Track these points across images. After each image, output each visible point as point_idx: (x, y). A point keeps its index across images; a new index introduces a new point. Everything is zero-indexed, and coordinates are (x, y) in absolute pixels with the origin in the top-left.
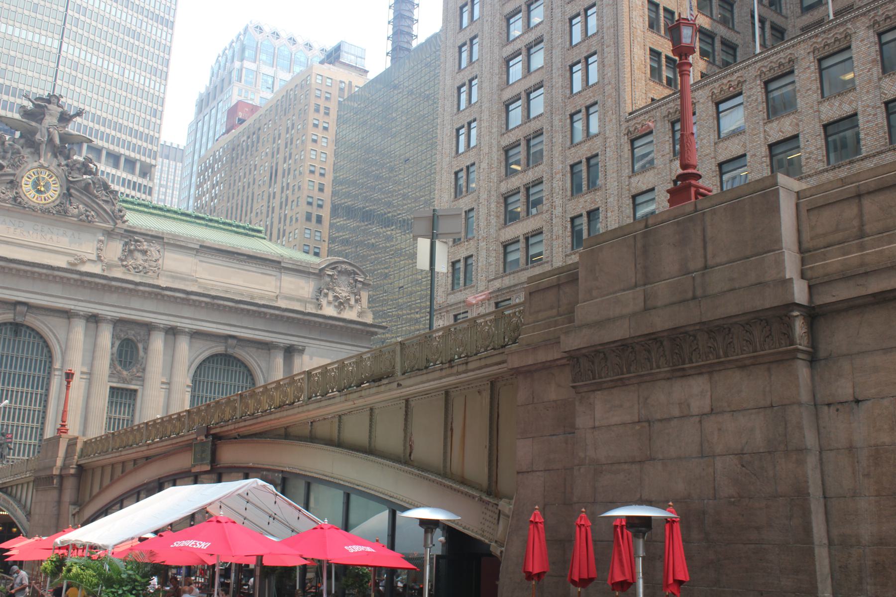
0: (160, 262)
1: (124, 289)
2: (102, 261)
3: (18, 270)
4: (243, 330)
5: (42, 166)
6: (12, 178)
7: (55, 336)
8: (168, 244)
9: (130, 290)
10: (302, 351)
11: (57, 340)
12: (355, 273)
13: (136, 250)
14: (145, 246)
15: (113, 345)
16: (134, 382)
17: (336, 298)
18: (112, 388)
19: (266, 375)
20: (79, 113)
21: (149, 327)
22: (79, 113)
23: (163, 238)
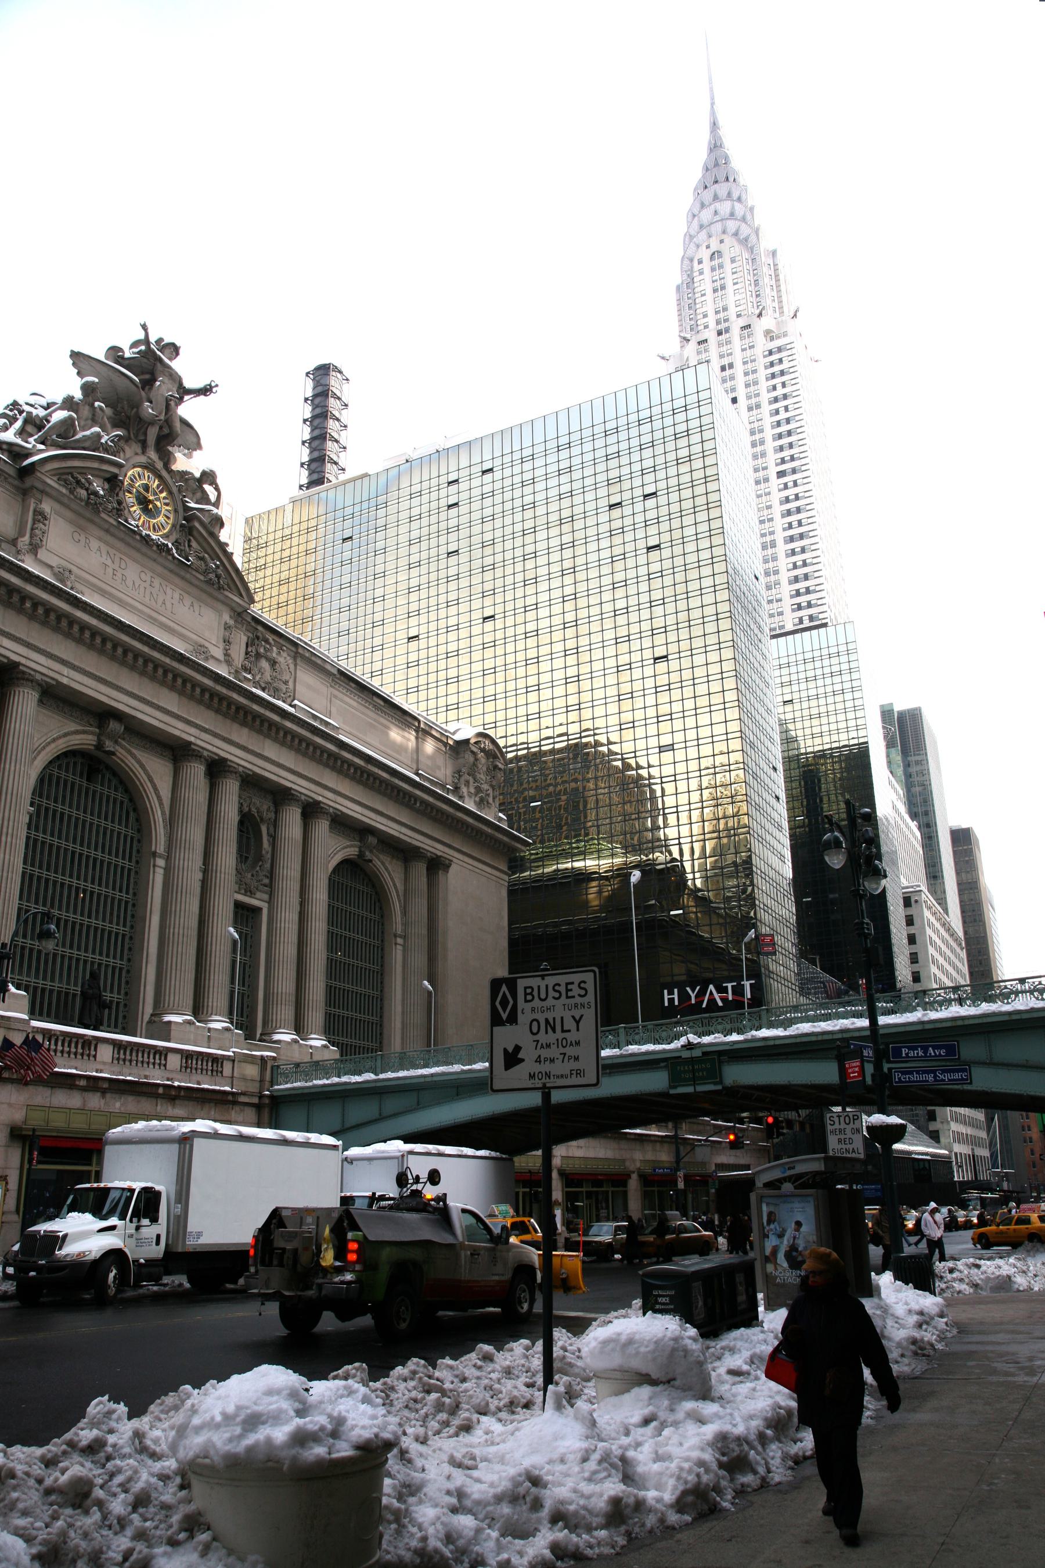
1: (263, 720)
3: (127, 650)
5: (149, 467)
6: (115, 470)
8: (303, 657)
9: (272, 724)
11: (159, 798)
12: (495, 757)
16: (258, 895)
17: (478, 790)
20: (206, 391)
22: (206, 391)
23: (295, 645)
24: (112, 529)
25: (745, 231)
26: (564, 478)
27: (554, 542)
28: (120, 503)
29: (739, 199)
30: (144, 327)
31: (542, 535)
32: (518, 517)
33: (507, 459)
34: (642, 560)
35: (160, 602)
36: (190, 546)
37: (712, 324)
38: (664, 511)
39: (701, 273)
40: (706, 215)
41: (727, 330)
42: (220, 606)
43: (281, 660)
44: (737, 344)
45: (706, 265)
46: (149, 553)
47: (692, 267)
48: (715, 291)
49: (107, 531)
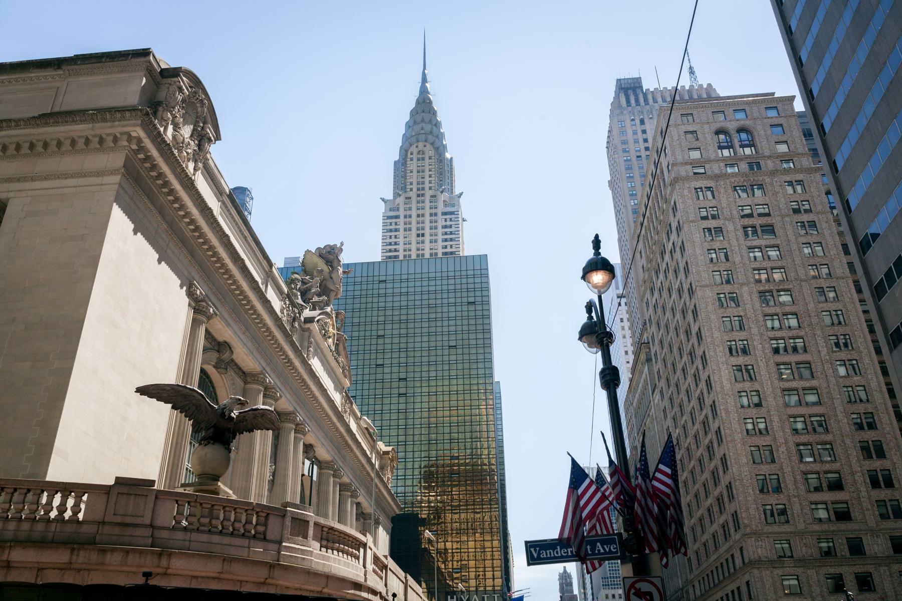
25: (437, 143)
26: (403, 298)
27: (396, 332)
29: (436, 125)
30: (342, 244)
31: (389, 327)
32: (375, 313)
33: (370, 279)
34: (446, 352)
37: (415, 190)
38: (459, 328)
39: (412, 159)
40: (417, 128)
41: (423, 195)
44: (427, 205)
45: (415, 157)
47: (406, 155)
48: (418, 172)
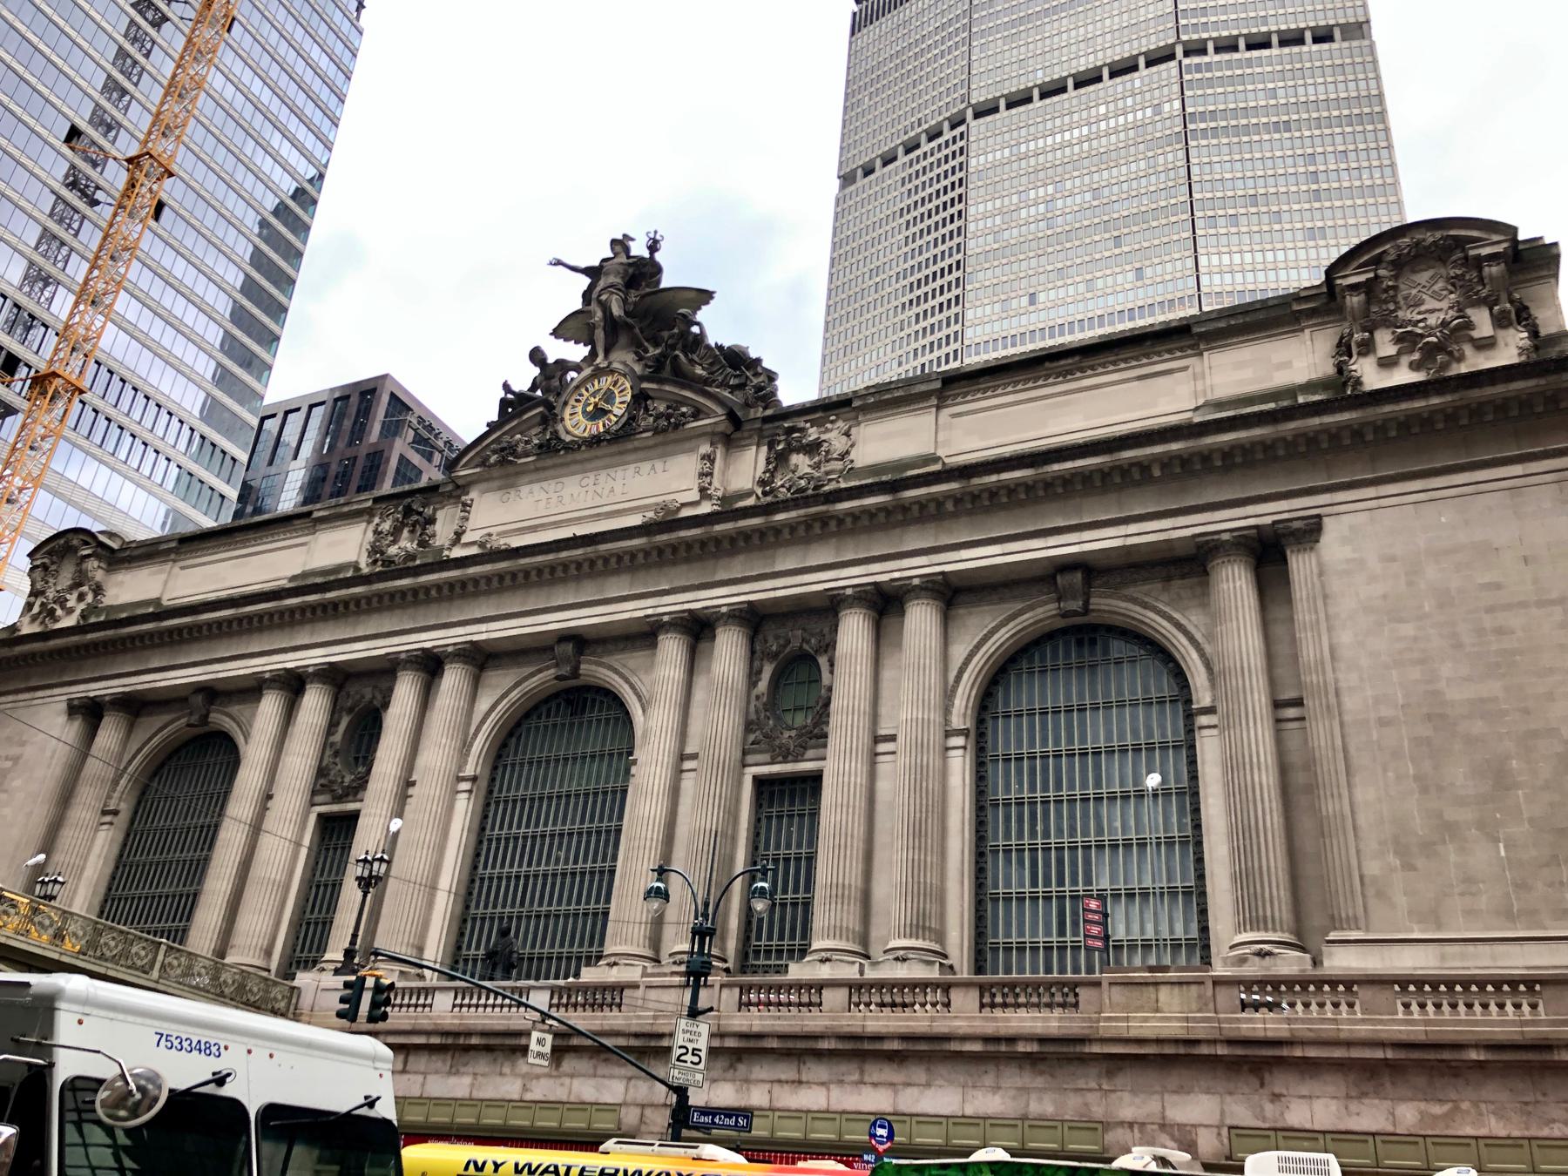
0: (852, 457)
2: (710, 497)
4: (1087, 535)
6: (541, 409)
7: (632, 687)
9: (761, 533)
10: (1310, 531)
12: (1461, 243)
13: (790, 450)
14: (813, 434)
15: (753, 676)
16: (810, 753)
17: (1407, 341)
18: (759, 781)
19: (1208, 649)
20: (654, 246)
21: (829, 607)
22: (654, 246)
24: (539, 465)
28: (555, 434)
30: (559, 263)
35: (606, 492)
36: (647, 409)
42: (693, 443)
43: (823, 437)
46: (586, 455)
49: (537, 470)
